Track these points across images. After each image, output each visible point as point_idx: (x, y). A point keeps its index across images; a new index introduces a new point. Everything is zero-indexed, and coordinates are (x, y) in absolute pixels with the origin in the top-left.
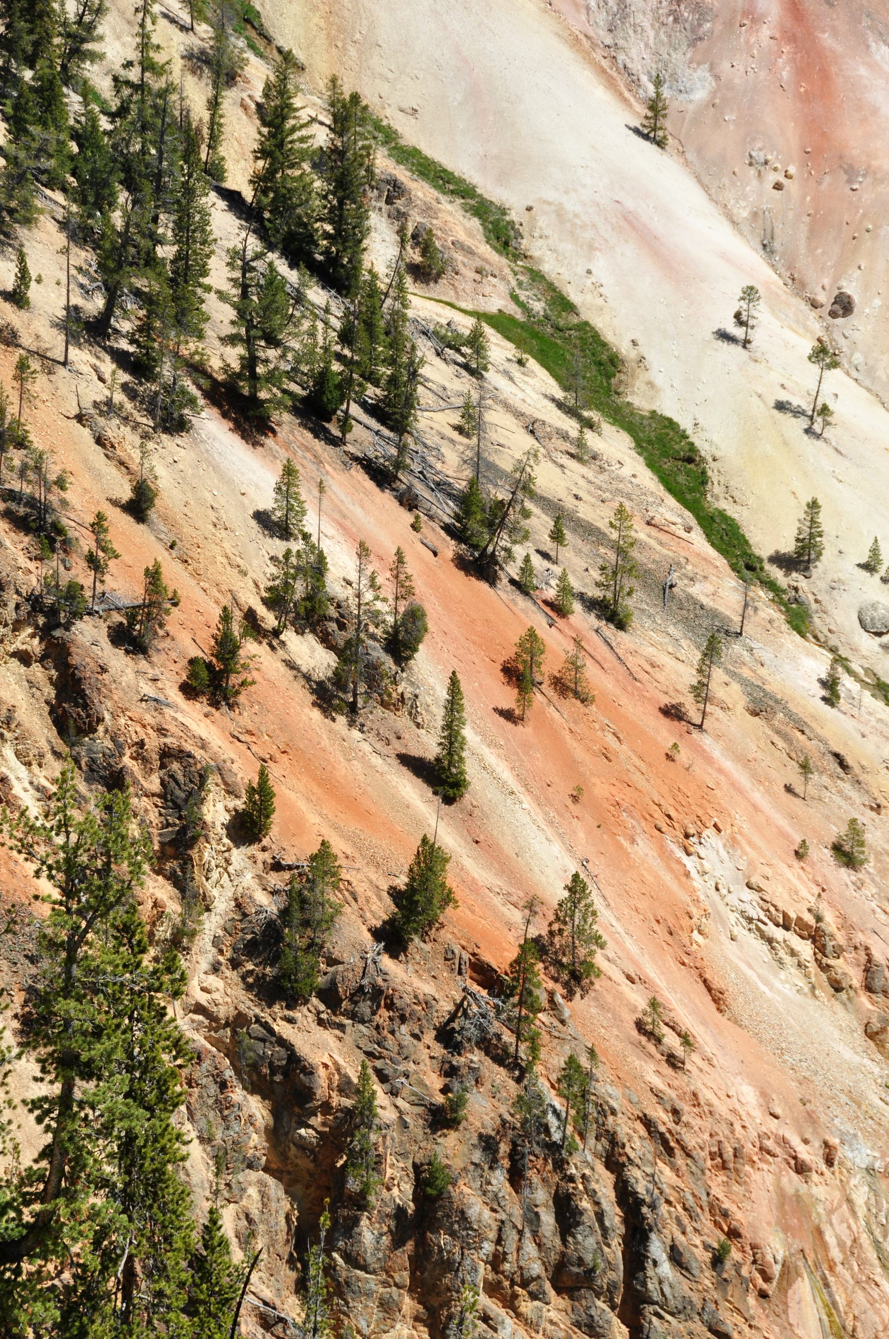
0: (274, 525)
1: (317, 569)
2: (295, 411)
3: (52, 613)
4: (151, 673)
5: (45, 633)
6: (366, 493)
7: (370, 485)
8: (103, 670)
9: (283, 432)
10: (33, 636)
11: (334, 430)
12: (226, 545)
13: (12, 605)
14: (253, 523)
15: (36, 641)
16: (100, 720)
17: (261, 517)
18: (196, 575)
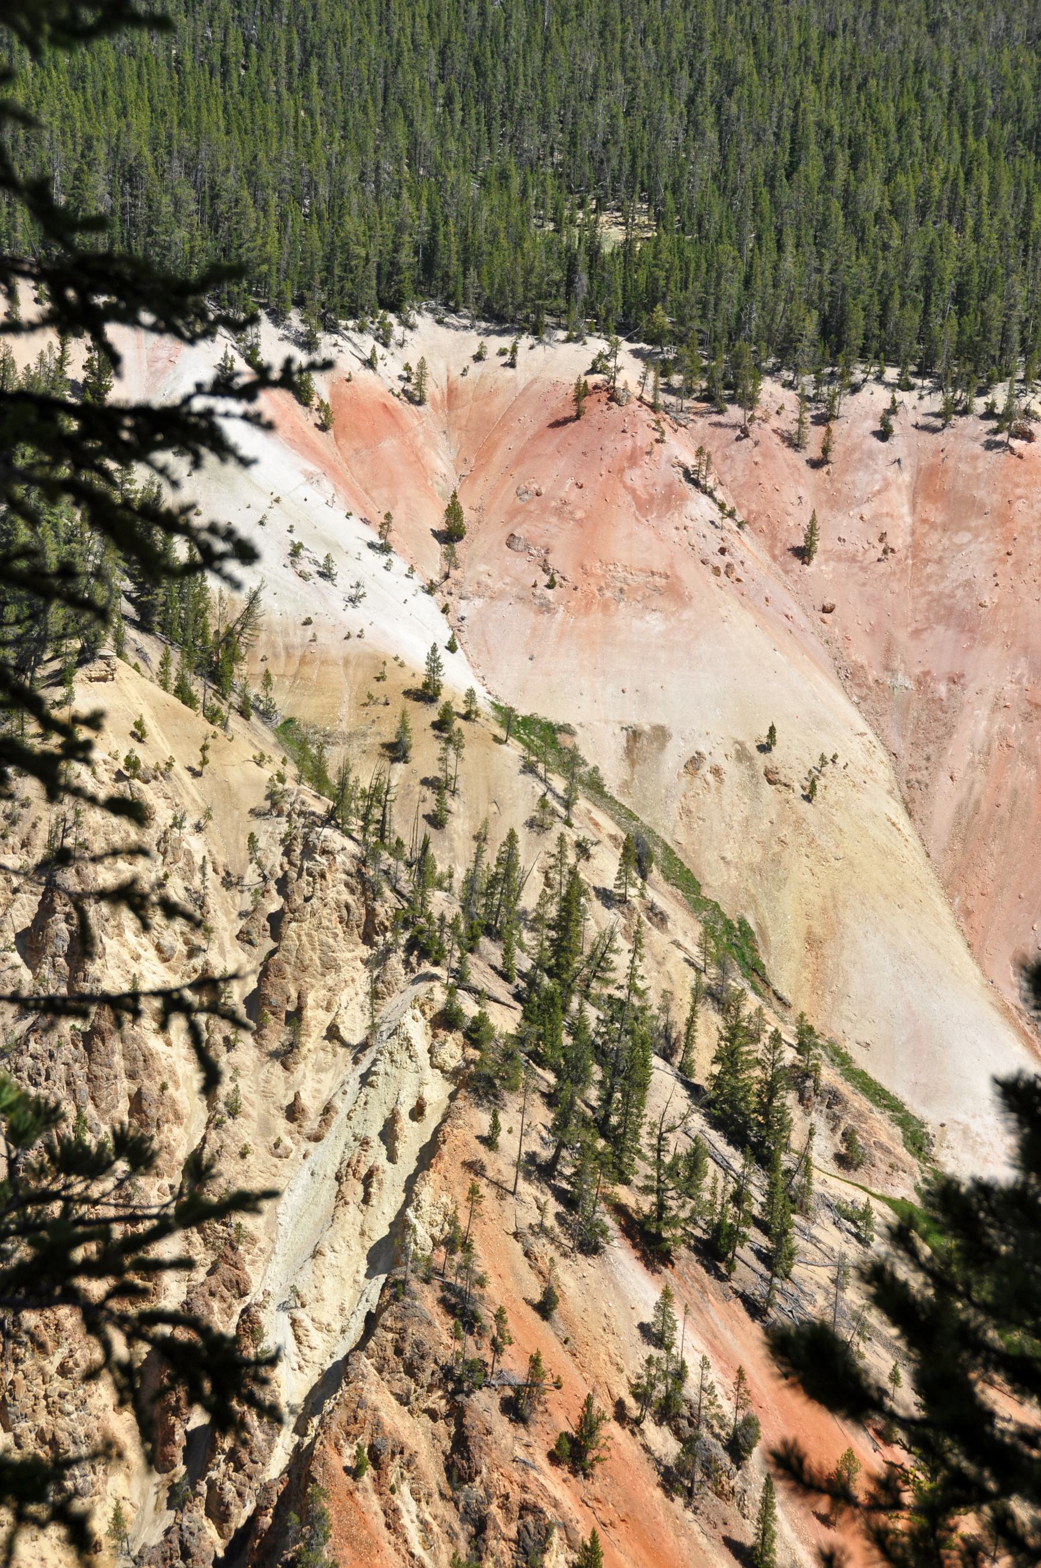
0: (655, 1335)
1: (680, 1375)
2: (695, 1250)
3: (459, 1381)
4: (526, 1439)
5: (450, 1397)
6: (738, 1320)
7: (743, 1315)
8: (489, 1432)
9: (679, 1265)
10: (441, 1398)
11: (722, 1267)
12: (611, 1346)
13: (429, 1372)
14: (637, 1332)
15: (443, 1402)
16: (478, 1472)
17: (644, 1328)
18: (581, 1367)
